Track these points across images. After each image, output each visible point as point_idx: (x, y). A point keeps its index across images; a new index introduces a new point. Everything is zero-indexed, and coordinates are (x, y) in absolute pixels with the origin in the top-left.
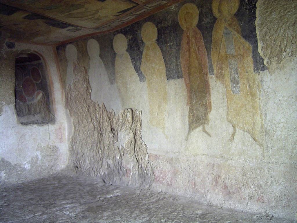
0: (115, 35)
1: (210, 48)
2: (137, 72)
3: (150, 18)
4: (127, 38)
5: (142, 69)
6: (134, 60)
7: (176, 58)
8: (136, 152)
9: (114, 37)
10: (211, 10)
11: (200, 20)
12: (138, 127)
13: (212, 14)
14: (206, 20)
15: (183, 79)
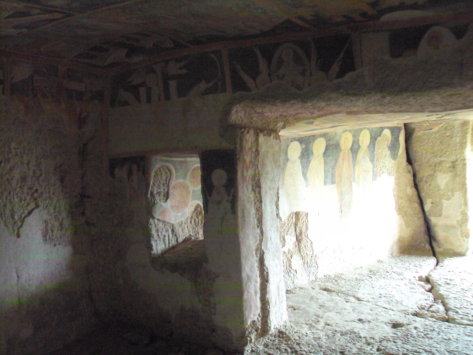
0: (292, 141)
1: (355, 164)
2: (304, 178)
3: (324, 135)
4: (301, 146)
5: (308, 175)
6: (303, 167)
7: (333, 168)
8: (302, 250)
9: (290, 143)
10: (358, 140)
11: (353, 146)
12: (304, 228)
13: (359, 144)
14: (356, 146)
15: (336, 185)
